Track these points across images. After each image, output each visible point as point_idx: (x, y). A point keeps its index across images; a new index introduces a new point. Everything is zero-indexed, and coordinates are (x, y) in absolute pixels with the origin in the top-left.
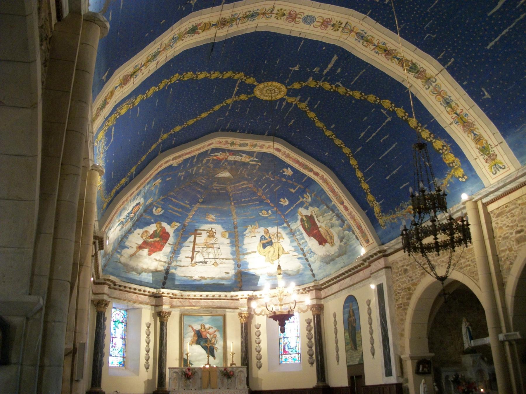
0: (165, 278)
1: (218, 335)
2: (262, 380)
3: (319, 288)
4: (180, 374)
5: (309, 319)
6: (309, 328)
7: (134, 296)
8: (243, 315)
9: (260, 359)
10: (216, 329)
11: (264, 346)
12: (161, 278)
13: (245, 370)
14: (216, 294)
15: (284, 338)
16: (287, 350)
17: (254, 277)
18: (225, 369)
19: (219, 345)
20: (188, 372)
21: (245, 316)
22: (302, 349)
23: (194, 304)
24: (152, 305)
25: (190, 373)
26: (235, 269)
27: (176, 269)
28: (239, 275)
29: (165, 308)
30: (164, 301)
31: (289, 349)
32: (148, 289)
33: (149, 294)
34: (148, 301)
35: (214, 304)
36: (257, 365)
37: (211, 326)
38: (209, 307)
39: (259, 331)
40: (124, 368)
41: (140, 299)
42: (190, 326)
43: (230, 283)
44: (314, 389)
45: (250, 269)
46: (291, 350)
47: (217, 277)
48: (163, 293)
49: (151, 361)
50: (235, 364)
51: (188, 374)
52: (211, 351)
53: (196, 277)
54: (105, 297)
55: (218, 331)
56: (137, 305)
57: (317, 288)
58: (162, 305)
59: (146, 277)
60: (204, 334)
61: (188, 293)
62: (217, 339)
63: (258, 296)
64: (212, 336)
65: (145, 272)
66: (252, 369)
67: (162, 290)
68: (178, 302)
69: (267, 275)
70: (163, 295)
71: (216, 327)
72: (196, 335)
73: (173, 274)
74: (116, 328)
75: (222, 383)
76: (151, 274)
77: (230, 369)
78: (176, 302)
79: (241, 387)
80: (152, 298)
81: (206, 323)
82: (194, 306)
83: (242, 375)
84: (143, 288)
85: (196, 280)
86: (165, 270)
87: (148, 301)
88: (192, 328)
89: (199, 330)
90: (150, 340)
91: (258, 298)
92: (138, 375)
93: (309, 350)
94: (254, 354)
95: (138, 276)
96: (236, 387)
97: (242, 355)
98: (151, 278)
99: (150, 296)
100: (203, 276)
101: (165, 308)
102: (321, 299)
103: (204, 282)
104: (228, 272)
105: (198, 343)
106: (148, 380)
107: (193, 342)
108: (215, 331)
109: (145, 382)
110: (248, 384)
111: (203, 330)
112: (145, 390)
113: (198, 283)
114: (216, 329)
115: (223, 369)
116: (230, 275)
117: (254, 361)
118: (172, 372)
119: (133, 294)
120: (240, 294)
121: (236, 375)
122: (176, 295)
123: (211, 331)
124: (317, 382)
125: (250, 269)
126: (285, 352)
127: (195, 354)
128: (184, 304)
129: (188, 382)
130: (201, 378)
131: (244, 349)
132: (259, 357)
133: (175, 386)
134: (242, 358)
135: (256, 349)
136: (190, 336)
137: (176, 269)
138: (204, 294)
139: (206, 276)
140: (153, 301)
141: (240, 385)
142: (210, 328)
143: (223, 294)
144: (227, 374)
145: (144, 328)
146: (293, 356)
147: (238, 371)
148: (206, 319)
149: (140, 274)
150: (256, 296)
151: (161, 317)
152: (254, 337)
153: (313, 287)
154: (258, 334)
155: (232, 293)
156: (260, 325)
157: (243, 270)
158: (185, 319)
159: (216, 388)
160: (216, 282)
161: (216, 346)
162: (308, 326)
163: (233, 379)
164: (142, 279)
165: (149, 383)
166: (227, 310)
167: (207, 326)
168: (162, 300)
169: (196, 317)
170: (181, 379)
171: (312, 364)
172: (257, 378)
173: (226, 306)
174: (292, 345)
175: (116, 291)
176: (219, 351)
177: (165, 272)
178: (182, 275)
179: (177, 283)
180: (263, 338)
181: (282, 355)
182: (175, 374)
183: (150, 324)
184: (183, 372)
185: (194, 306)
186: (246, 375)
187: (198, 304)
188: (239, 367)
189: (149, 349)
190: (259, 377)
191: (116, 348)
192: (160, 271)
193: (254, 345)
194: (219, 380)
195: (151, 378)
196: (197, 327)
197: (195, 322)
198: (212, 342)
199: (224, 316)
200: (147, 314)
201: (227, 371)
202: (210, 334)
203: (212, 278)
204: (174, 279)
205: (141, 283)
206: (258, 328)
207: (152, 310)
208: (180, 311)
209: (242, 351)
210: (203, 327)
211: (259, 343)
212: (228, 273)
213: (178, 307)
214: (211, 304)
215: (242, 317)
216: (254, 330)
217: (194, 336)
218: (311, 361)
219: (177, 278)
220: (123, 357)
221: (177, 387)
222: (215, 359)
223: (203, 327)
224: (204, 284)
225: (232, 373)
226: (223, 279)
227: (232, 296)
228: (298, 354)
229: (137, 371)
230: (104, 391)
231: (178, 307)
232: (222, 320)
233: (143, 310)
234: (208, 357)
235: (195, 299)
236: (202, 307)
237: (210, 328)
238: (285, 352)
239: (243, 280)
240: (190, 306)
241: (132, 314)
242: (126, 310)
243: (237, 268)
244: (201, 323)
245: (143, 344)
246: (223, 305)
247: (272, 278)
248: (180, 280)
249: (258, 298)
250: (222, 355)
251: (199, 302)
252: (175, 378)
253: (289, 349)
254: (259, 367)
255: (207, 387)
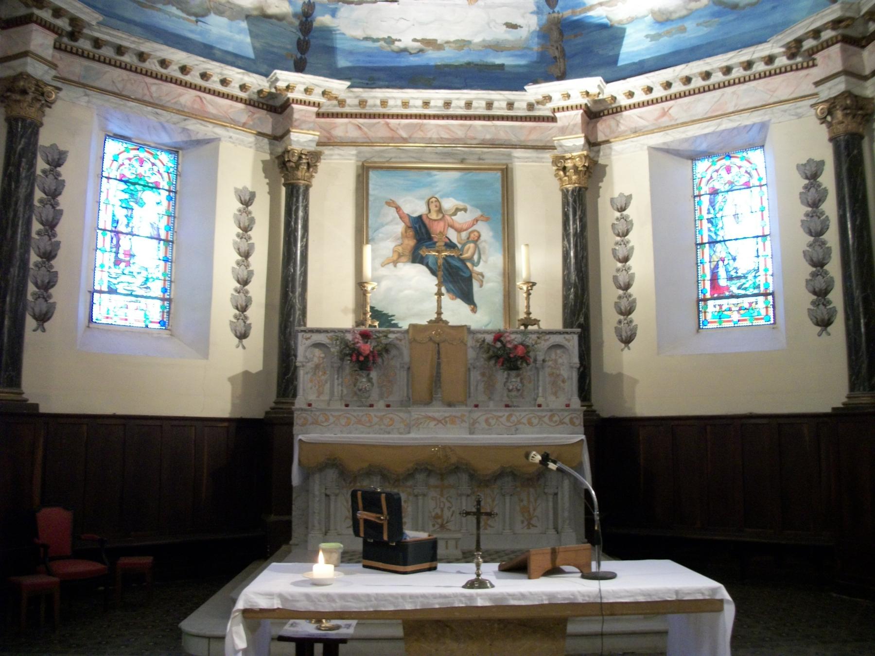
0: (303, 46)
1: (486, 232)
2: (635, 382)
3: (855, 32)
4: (334, 350)
5: (810, 161)
6: (812, 194)
7: (188, 97)
8: (569, 164)
9: (629, 312)
10: (478, 213)
11: (642, 265)
12: (288, 42)
13: (572, 342)
14: (478, 97)
15: (713, 243)
16: (723, 282)
17: (605, 33)
18: (499, 337)
19: (488, 267)
20: (361, 344)
21: (575, 168)
22: (784, 272)
23: (405, 135)
24: (260, 134)
25: (366, 348)
26: (538, 12)
27: (333, 13)
28: (555, 34)
29: (301, 139)
30: (296, 116)
31: (730, 278)
32: (237, 76)
33: (244, 95)
34: (244, 118)
35: (471, 134)
36: (618, 331)
37: (460, 204)
38: (456, 141)
39: (625, 218)
40: (165, 334)
41: (211, 110)
42: (391, 203)
43: (523, 62)
44: (837, 415)
45: (591, 8)
46: (739, 283)
47: (477, 40)
48: (288, 88)
49: (257, 315)
50: (536, 322)
51: (367, 351)
52: (457, 279)
53: (406, 41)
54: (37, 70)
55: (485, 218)
56: (200, 129)
57: (849, 32)
58: (288, 132)
59: (226, 33)
60: (436, 228)
61: (379, 94)
62: (482, 245)
63: (623, 101)
64: (464, 235)
65: (220, 13)
66: (601, 345)
67: (285, 77)
68: (351, 128)
69: (649, 19)
70: (290, 95)
71: (477, 207)
72: (411, 233)
73: (328, 32)
74: (133, 204)
75: (490, 388)
76: (244, 25)
77: (517, 339)
78: (342, 128)
79: (556, 402)
80: (262, 114)
81: (447, 195)
82: (405, 140)
83: (563, 360)
84: (216, 69)
85: (405, 50)
86: (295, 15)
87: (244, 118)
88: (398, 209)
89: (420, 217)
90: (251, 247)
91: (619, 110)
92: (206, 355)
93: (814, 275)
94: (609, 295)
95: (193, 27)
96: (540, 400)
97: (565, 298)
98: (248, 40)
99: (249, 103)
100: (430, 36)
101: (301, 139)
102: (865, 78)
103: (433, 57)
104: (514, 23)
105: (416, 258)
106: (246, 375)
107: (400, 256)
108: (477, 220)
109: (232, 380)
110: (584, 392)
111: (434, 216)
112: (234, 405)
113: (414, 61)
114: (478, 213)
115: (489, 338)
116: (523, 34)
117: (608, 319)
118: (308, 343)
119: (180, 89)
120: (554, 89)
121: (540, 358)
122: (342, 103)
123: (461, 219)
124: (853, 387)
125: (591, 8)
126: (718, 291)
127: (407, 292)
128: (371, 134)
129: (363, 382)
130: (409, 368)
131: (573, 277)
132: (624, 304)
133: (320, 393)
134: (565, 306)
135: (615, 278)
136: (391, 233)
137: (333, 13)
138: (437, 96)
139: (439, 35)
140: (267, 122)
141: (555, 394)
142: (458, 210)
143: (500, 98)
144: (508, 355)
145: (227, 207)
146: (745, 302)
147: (544, 345)
148: (445, 180)
149: (200, 15)
150: (614, 99)
151: (289, 175)
152: (607, 240)
153: (836, 24)
154: (621, 227)
155: (534, 92)
156: (629, 198)
157: (567, 14)
158: (374, 177)
159: (464, 403)
160: (474, 58)
161: (478, 269)
162: (807, 188)
163: (527, 371)
164: (210, 40)
165: (247, 381)
166: (518, 153)
167: (448, 204)
168: (290, 117)
169: (412, 175)
170: (340, 369)
171: (824, 323)
172: (620, 376)
173: (514, 140)
174: (744, 265)
175: (107, 68)
176: (487, 285)
177: (297, 23)
178: (359, 33)
179: (342, 62)
180: (641, 240)
181: (705, 300)
182: (317, 352)
183: (253, 195)
184: (346, 344)
185: (405, 140)
186: (576, 360)
187: (420, 134)
188: (551, 333)
189: (251, 273)
190: (627, 371)
191: (134, 268)
192: (279, 18)
193: (608, 267)
194: (475, 376)
195: (256, 365)
196: (415, 207)
197: (408, 189)
198: (465, 256)
199: (506, 174)
200: (240, 162)
201: (504, 346)
202: (459, 231)
203: (462, 44)
204: (330, 50)
205: (207, 51)
206: (622, 209)
207: (258, 149)
208: (358, 155)
209: (566, 283)
210: (433, 208)
211: (626, 260)
212: (514, 27)
213: (353, 143)
214: (460, 134)
215: (564, 169)
216: (607, 216)
217: (404, 236)
218: (822, 312)
219: (340, 44)
220: (163, 300)
221: (326, 397)
222: (474, 310)
223: (433, 208)
224: (436, 66)
225: (520, 351)
226: (496, 47)
227: (531, 107)
228: (766, 295)
229: (202, 344)
230: (31, 401)
231: (353, 143)
232: (498, 185)
233: (225, 148)
234: (439, 294)
235: (407, 116)
236: (430, 141)
237: (458, 210)
238: (718, 291)
239: (567, 49)
240: (392, 139)
241: (189, 158)
242: (174, 151)
243: (547, 9)
244: (426, 193)
245: (225, 258)
246: (503, 136)
247: (668, 28)
248: (351, 53)
249: (619, 110)
250: (499, 299)
251: (422, 125)
252: (317, 367)
253: (730, 278)
254: (627, 341)
255: (428, 402)
